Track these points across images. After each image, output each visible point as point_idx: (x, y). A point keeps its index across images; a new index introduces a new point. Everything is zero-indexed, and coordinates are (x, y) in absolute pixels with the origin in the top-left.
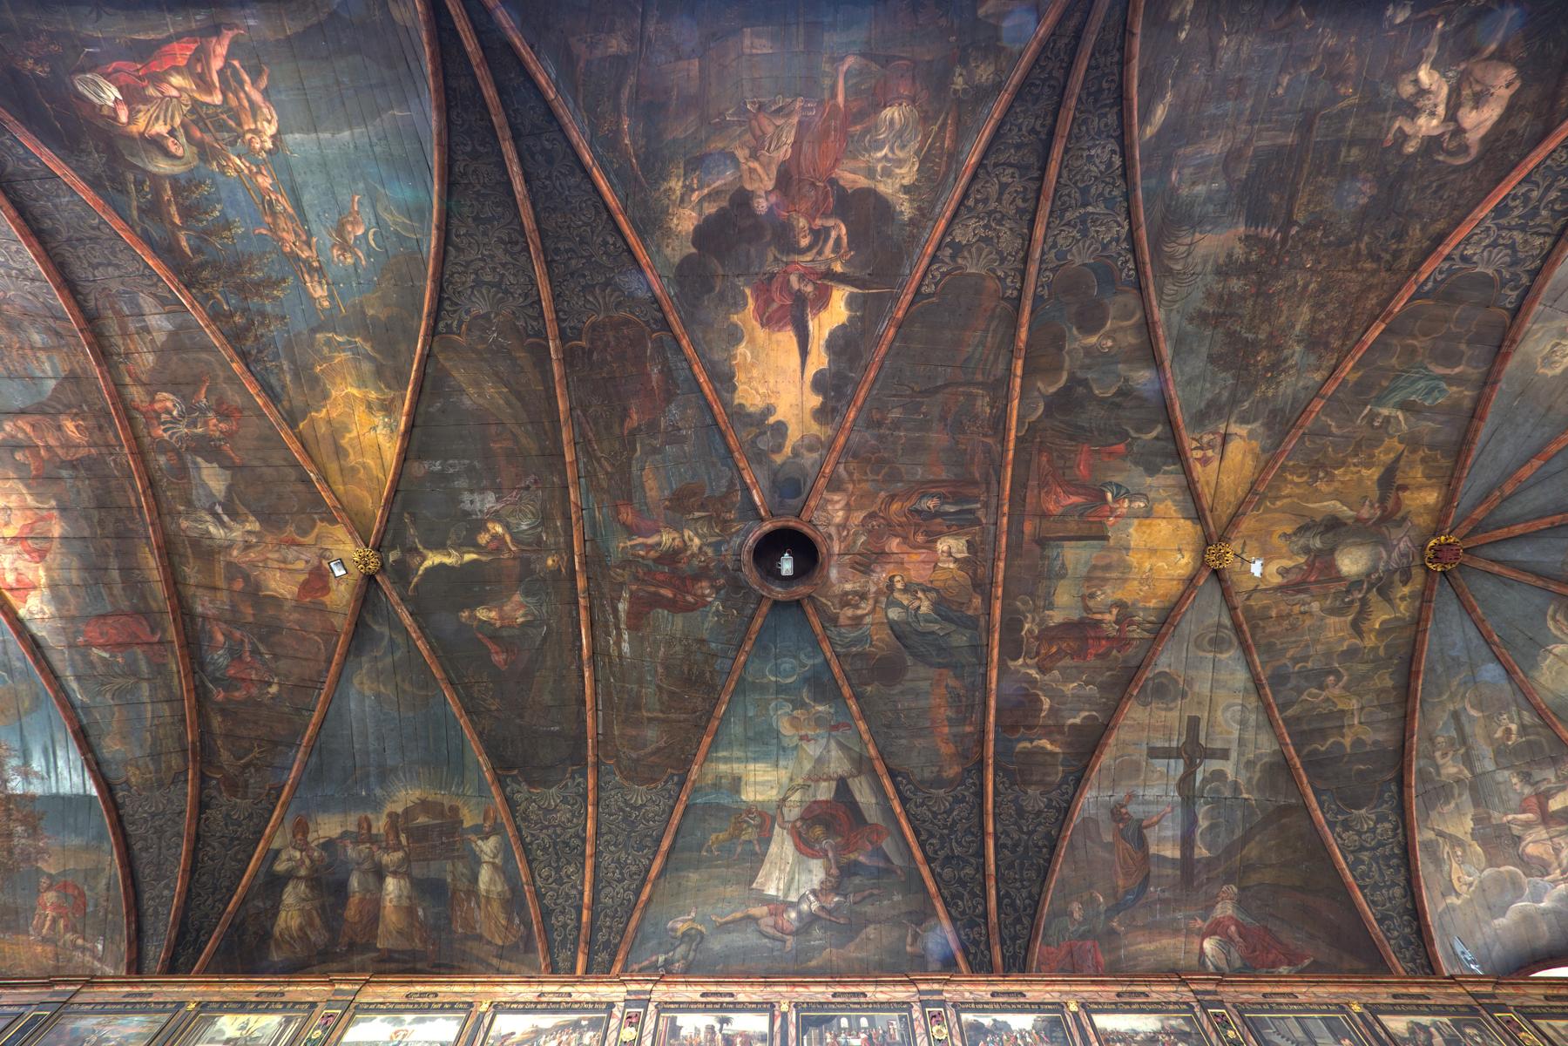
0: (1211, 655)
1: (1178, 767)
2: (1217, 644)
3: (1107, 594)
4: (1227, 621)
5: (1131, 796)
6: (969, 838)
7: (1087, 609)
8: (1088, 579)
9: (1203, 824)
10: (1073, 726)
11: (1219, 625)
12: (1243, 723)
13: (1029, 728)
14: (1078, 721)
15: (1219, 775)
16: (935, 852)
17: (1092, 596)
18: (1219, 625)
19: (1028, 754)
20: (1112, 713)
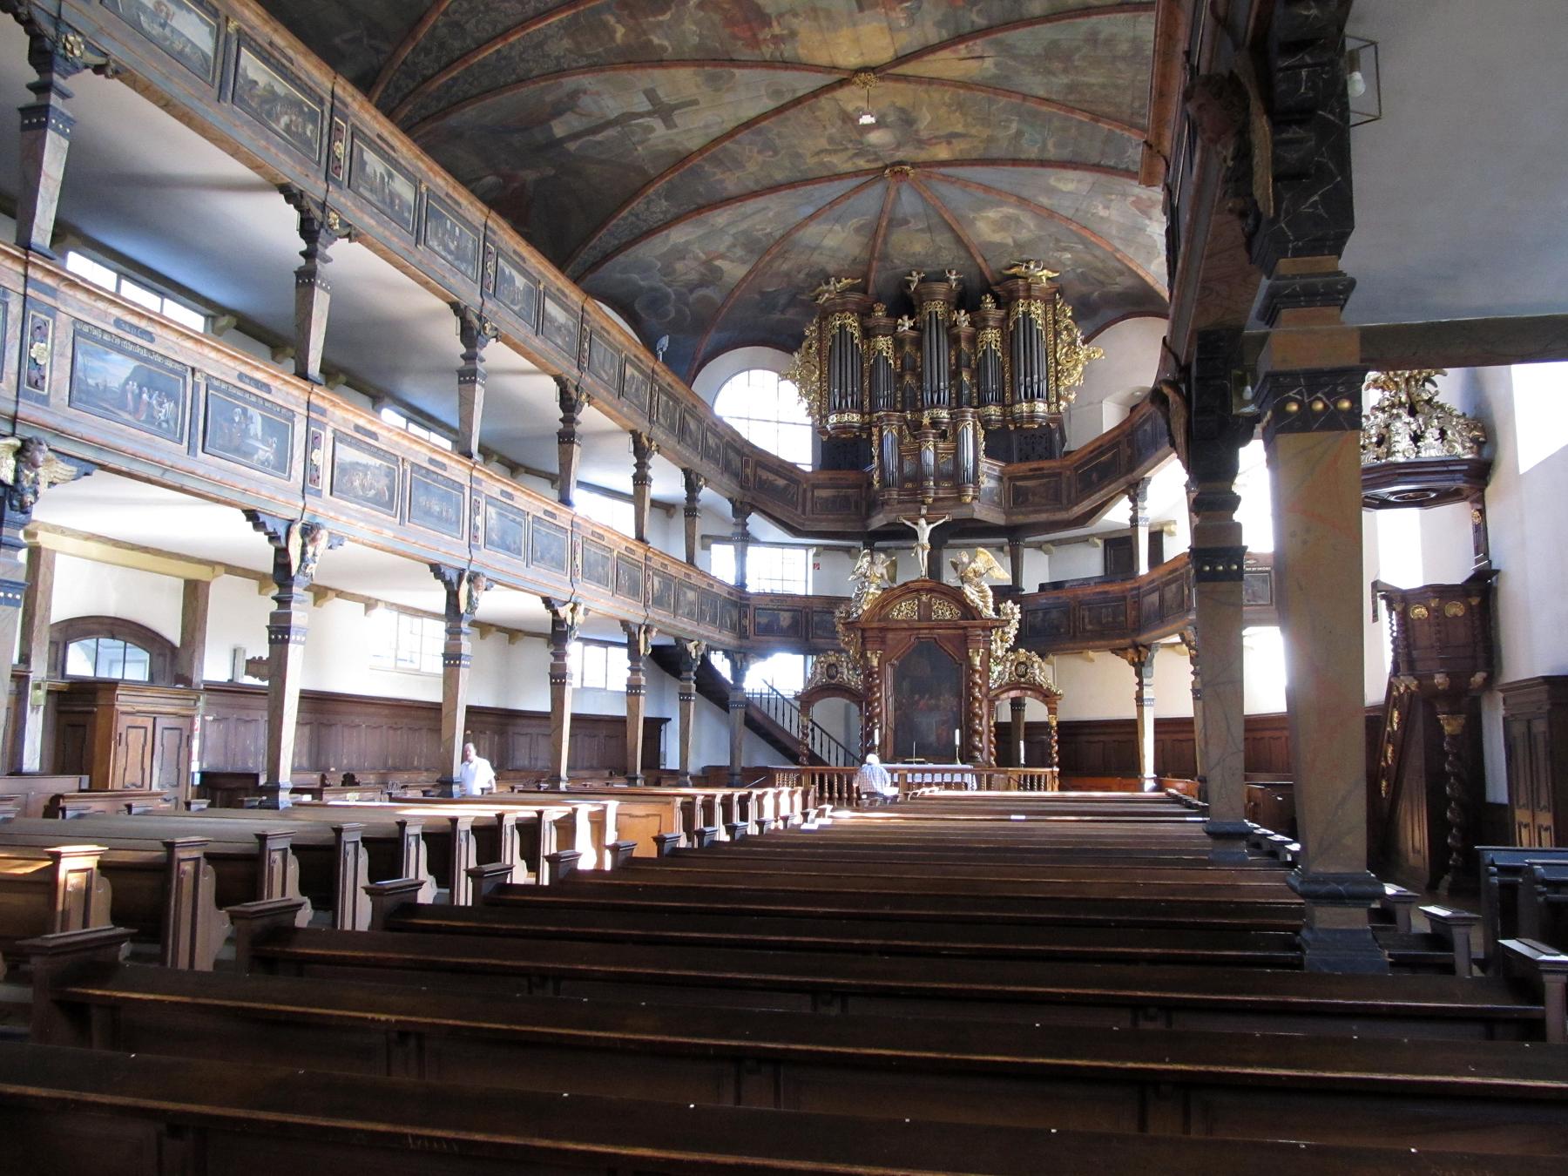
0: (763, 92)
1: (646, 106)
2: (777, 93)
3: (802, 25)
4: (800, 94)
5: (598, 93)
6: (489, 27)
7: (781, 15)
8: (814, 10)
9: (599, 137)
10: (650, 41)
11: (794, 91)
12: (706, 126)
13: (632, 16)
14: (656, 41)
15: (651, 129)
16: (455, 12)
17: (796, 15)
18: (794, 91)
19: (605, 25)
20: (680, 62)
